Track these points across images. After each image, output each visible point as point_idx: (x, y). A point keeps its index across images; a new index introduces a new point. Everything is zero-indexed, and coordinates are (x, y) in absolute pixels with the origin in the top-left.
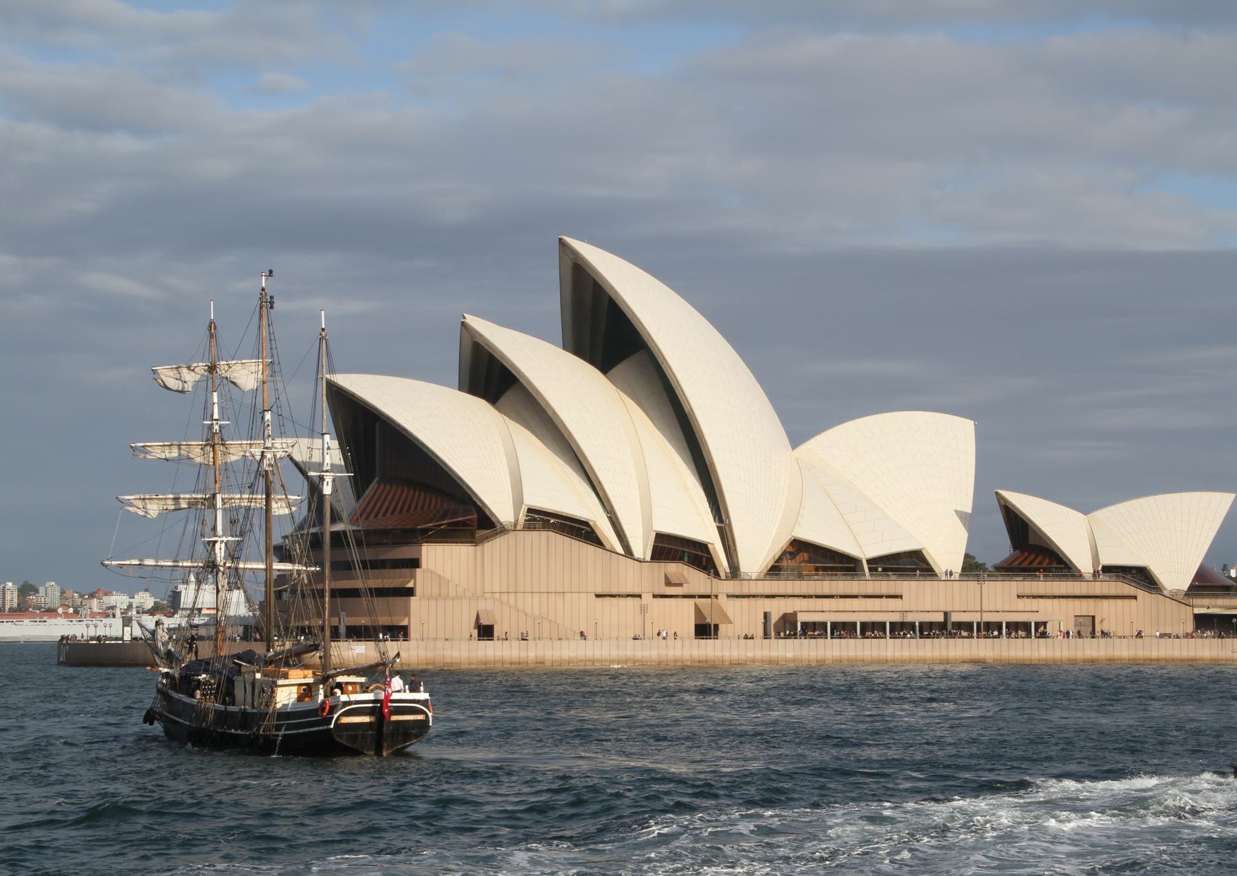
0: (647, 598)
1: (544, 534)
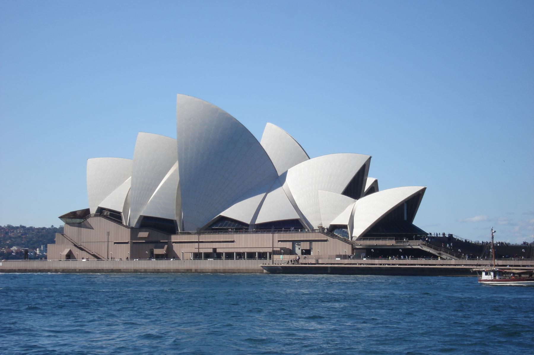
1: (99, 218)
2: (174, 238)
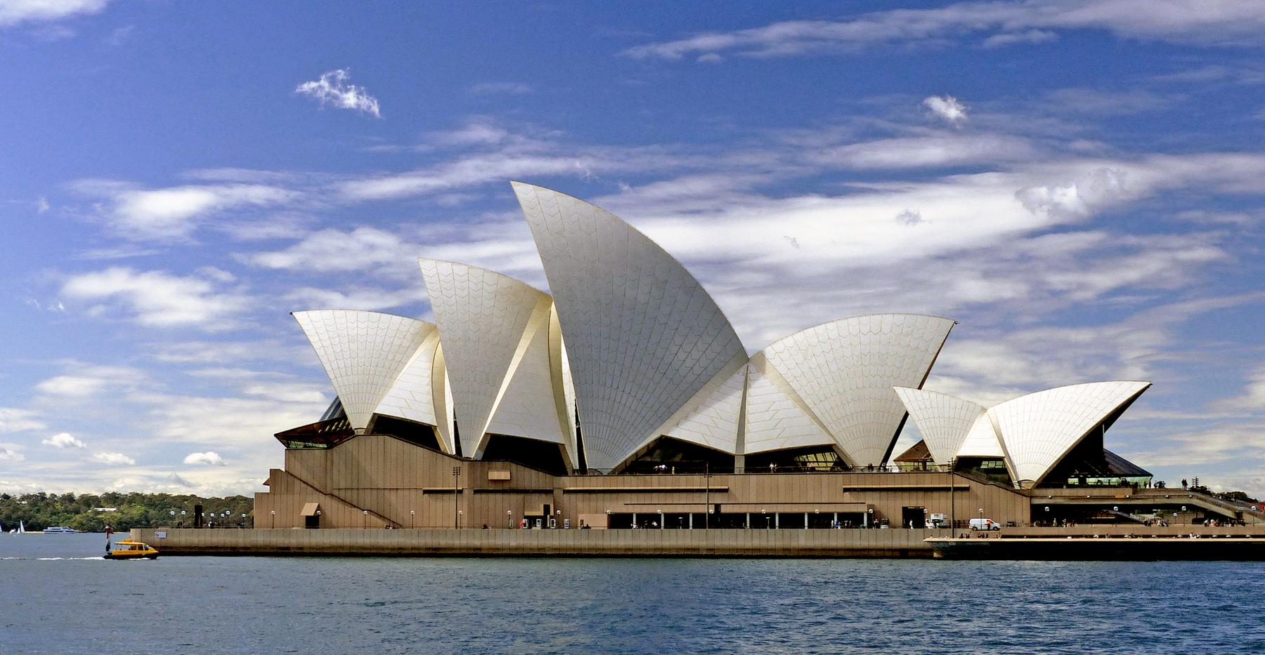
0: (466, 492)
1: (381, 438)
2: (568, 483)
